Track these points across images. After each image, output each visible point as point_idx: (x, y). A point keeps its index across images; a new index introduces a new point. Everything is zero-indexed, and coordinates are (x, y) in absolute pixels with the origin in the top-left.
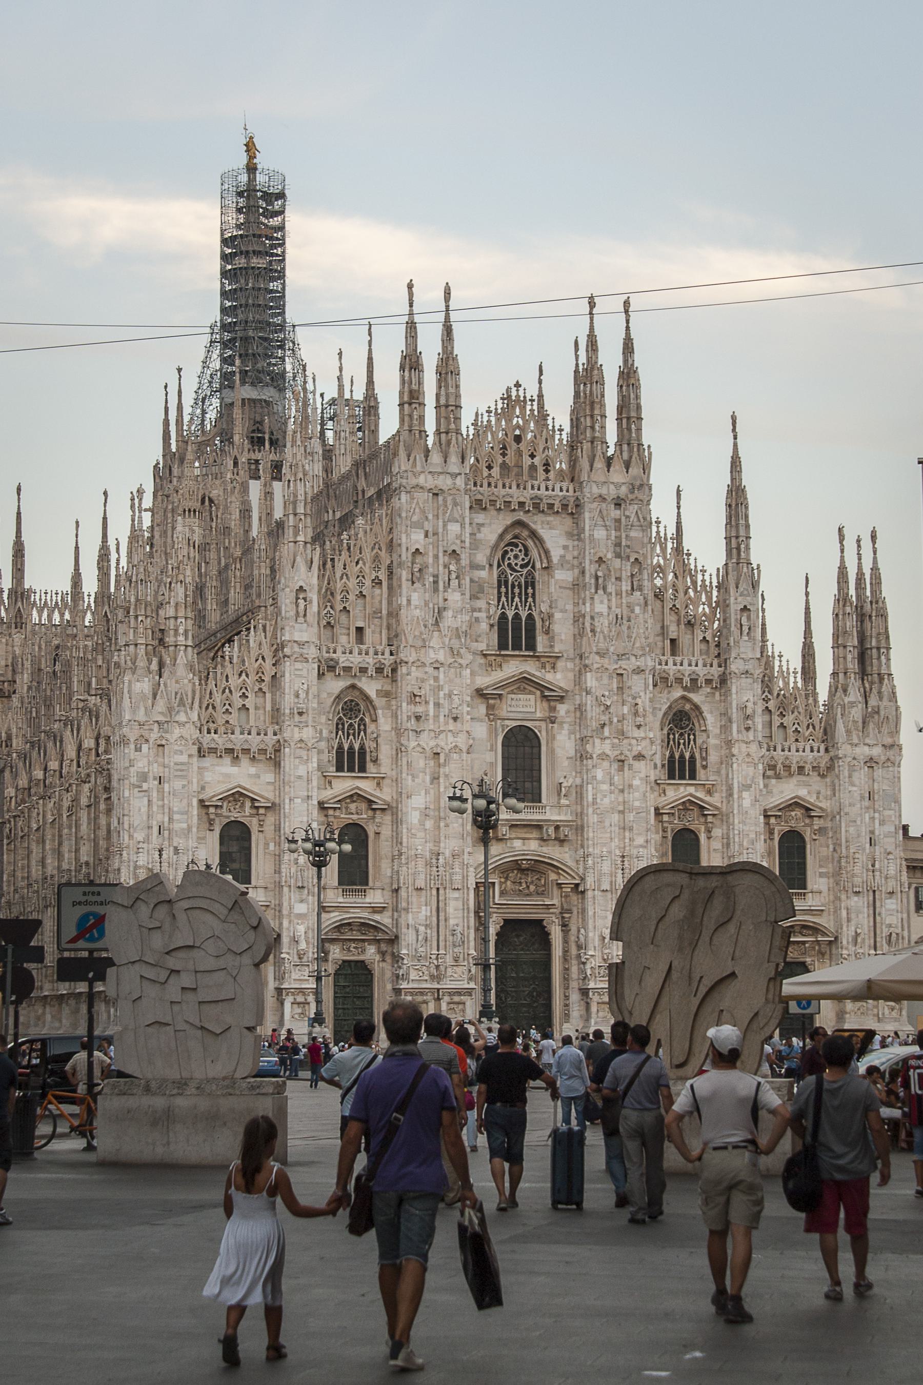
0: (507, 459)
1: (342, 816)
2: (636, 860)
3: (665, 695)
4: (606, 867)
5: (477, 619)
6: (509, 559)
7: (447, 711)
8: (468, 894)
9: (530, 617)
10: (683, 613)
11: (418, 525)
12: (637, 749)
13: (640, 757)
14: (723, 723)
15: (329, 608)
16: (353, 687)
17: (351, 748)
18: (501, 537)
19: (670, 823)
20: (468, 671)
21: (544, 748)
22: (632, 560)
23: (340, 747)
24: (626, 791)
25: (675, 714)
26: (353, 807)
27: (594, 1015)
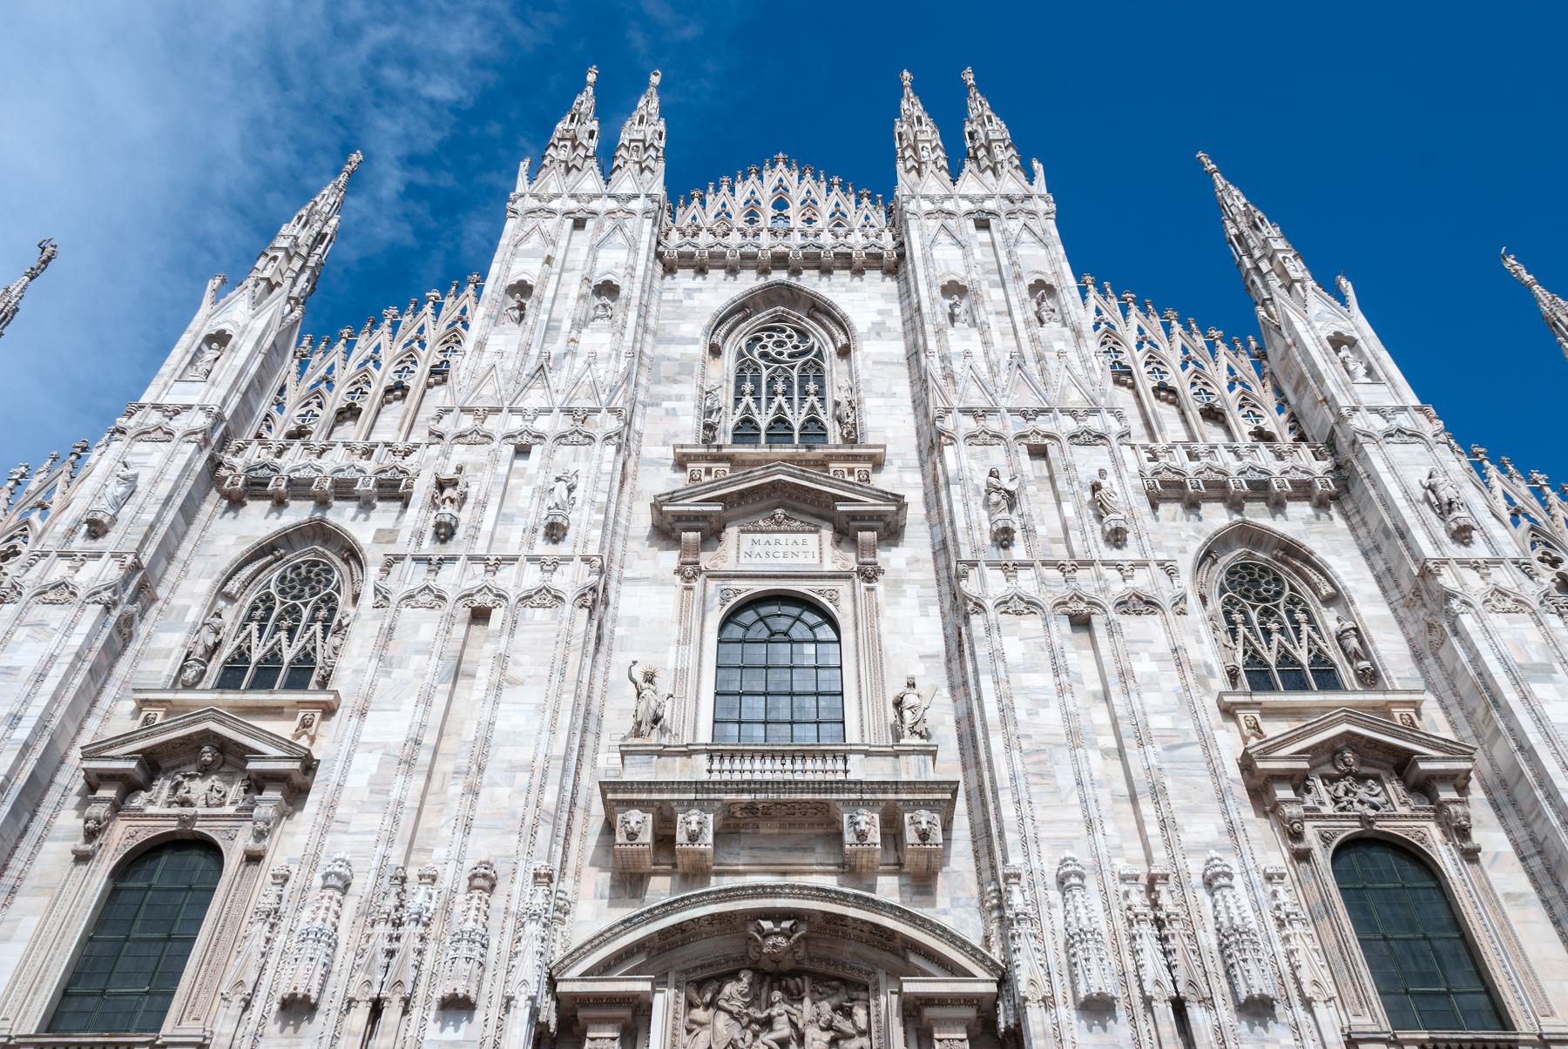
1: (150, 810)
2: (1202, 893)
5: (672, 413)
6: (764, 347)
7: (531, 521)
10: (1187, 392)
11: (530, 254)
14: (1381, 566)
15: (314, 406)
17: (274, 657)
19: (1313, 814)
22: (1030, 280)
23: (242, 655)
24: (1115, 689)
25: (1231, 572)
26: (198, 788)
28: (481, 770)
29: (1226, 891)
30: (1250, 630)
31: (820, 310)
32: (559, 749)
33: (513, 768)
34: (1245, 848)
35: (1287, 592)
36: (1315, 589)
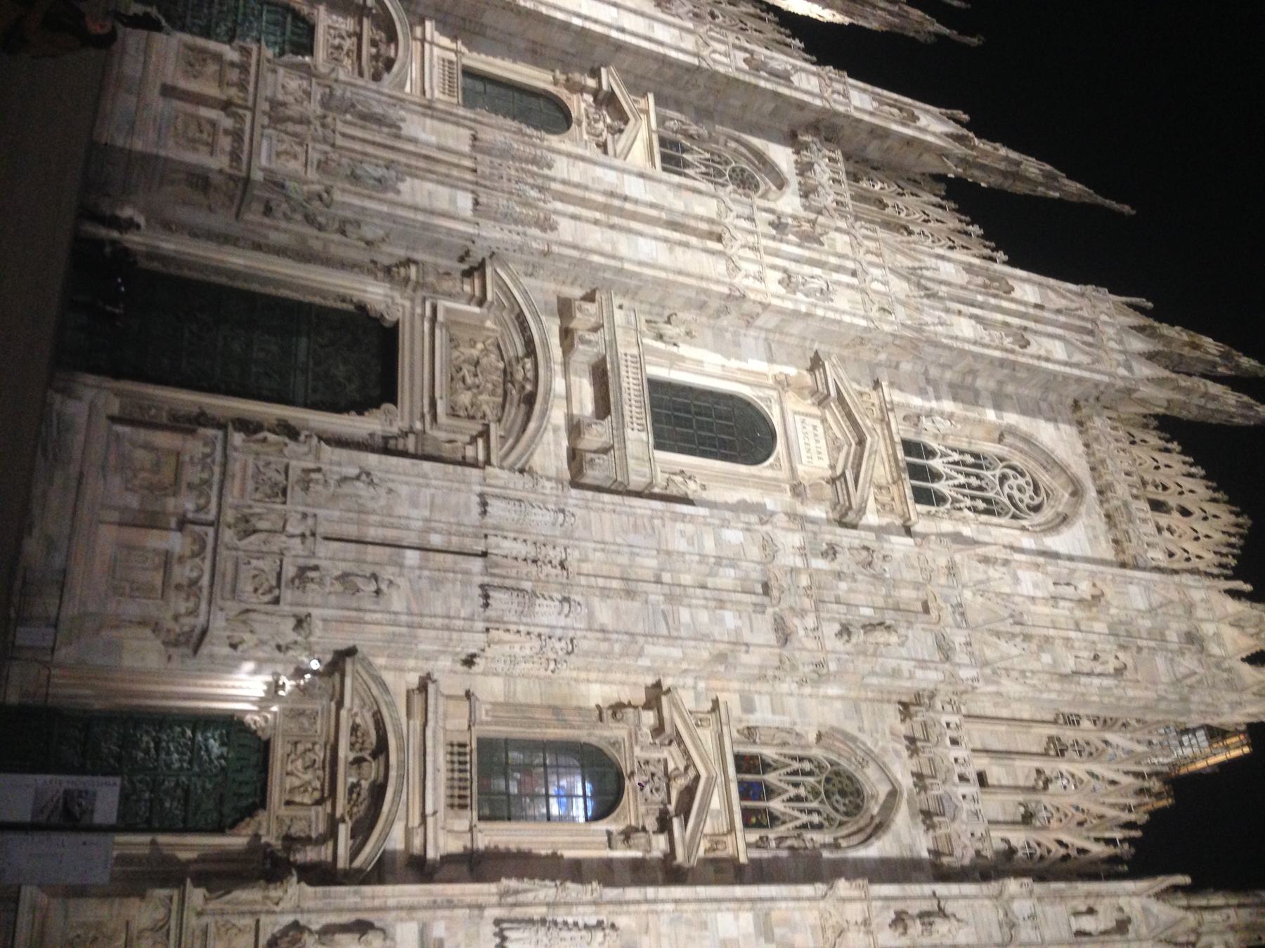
0: (1150, 488)
3: (892, 745)
4: (542, 520)
6: (1015, 478)
8: (465, 220)
9: (941, 499)
10: (1045, 799)
12: (795, 623)
13: (784, 635)
16: (781, 184)
18: (1050, 462)
19: (634, 737)
20: (863, 323)
21: (743, 469)
24: (708, 593)
25: (851, 778)
27: (143, 435)
28: (612, 227)
29: (558, 609)
30: (795, 773)
31: (1064, 520)
32: (627, 266)
33: (613, 244)
34: (589, 634)
35: (839, 817)
36: (843, 837)
